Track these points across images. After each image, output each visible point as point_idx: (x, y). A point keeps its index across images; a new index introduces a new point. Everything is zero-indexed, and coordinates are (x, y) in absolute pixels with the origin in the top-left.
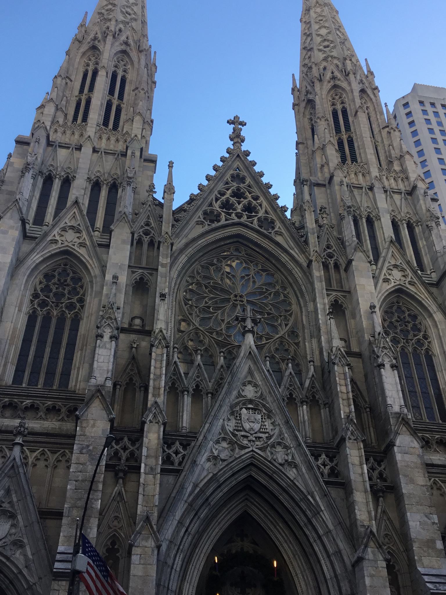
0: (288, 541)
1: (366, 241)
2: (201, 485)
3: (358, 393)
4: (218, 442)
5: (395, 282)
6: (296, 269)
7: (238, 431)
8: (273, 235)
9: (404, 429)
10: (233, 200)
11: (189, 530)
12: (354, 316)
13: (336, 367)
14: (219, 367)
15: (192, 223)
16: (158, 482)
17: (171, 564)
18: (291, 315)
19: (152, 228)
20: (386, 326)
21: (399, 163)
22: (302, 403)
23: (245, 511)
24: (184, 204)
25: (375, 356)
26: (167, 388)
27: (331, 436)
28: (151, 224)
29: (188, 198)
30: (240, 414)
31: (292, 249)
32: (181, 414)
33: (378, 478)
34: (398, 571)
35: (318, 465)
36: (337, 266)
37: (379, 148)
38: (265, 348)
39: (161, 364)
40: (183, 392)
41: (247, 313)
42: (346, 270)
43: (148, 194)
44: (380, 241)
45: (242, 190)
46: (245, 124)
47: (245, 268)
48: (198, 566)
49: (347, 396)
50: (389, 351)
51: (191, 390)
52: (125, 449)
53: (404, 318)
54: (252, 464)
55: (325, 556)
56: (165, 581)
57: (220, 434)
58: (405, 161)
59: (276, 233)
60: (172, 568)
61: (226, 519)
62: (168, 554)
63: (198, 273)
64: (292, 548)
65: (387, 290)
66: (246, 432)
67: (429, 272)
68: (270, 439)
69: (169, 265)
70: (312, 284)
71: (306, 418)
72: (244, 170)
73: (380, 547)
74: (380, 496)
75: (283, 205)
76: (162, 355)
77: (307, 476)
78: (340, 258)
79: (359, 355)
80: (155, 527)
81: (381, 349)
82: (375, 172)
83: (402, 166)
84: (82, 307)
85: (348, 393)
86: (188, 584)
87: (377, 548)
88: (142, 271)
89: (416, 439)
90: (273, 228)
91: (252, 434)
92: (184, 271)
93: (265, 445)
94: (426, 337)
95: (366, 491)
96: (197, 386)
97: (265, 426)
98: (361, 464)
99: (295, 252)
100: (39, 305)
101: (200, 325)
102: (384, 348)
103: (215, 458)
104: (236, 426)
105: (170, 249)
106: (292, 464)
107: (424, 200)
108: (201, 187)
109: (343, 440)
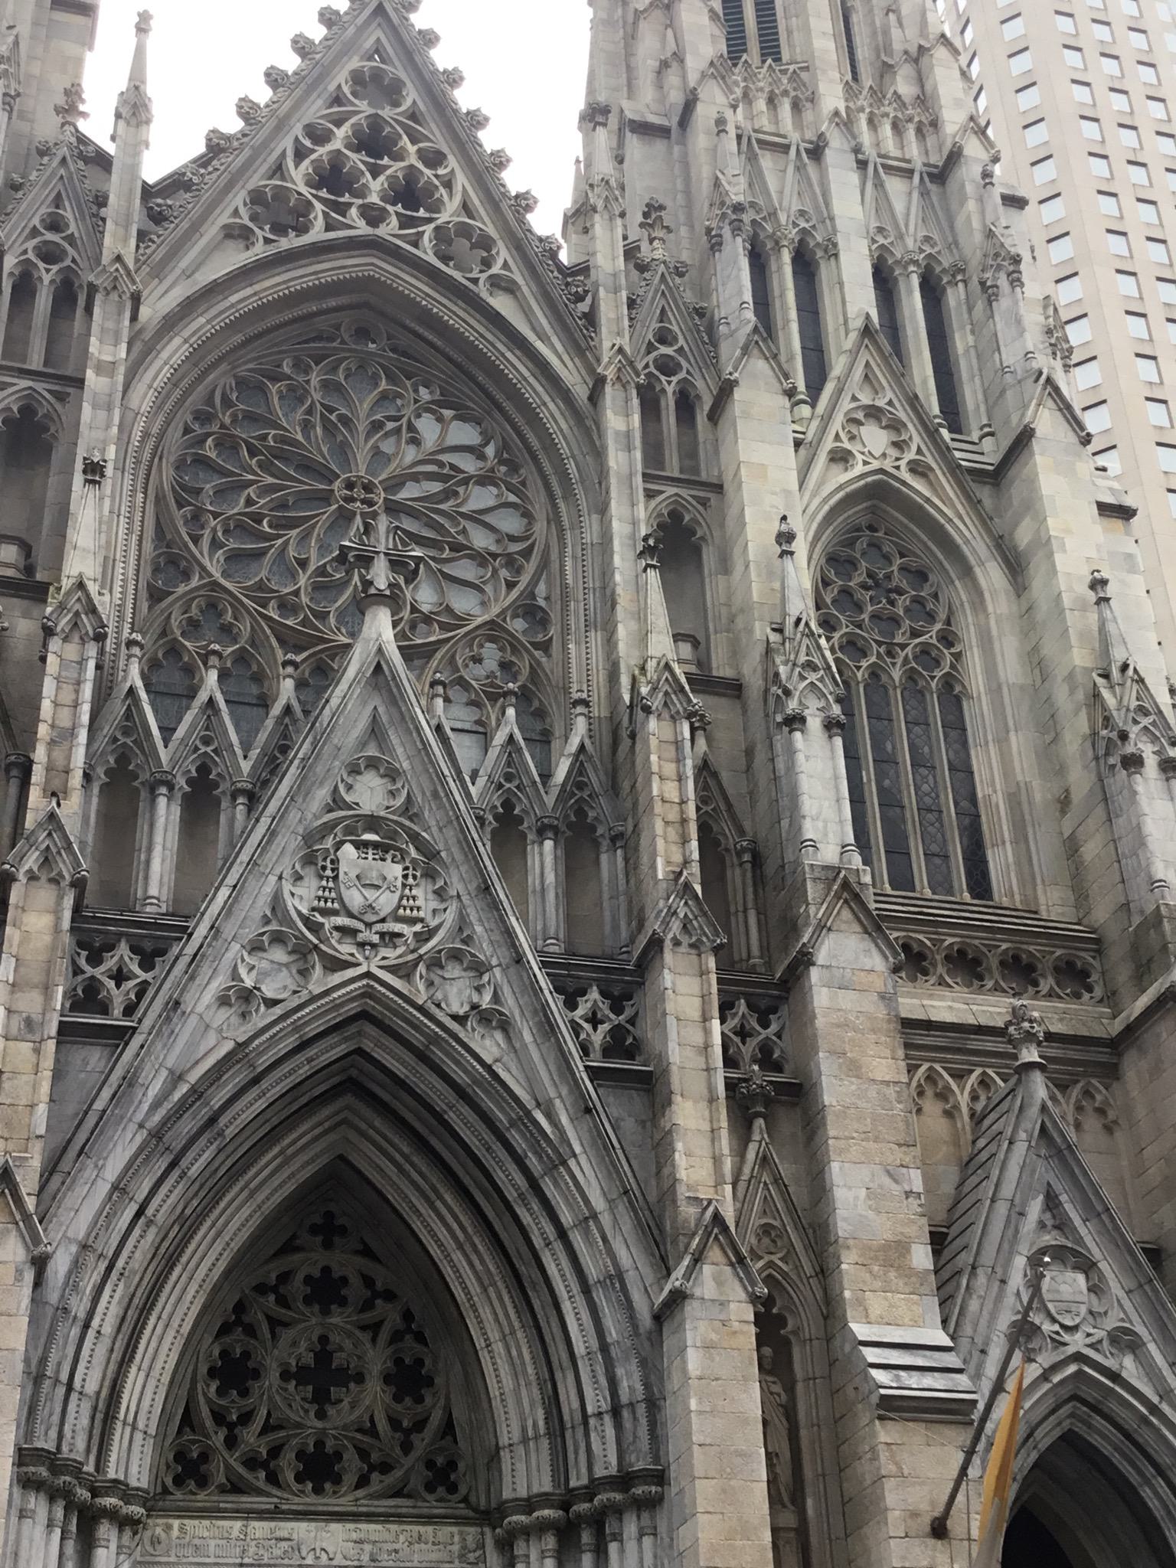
0: (468, 1248)
1: (787, 321)
2: (194, 1077)
3: (723, 807)
4: (256, 947)
5: (865, 463)
6: (551, 406)
7: (325, 912)
8: (483, 290)
9: (846, 914)
10: (357, 160)
11: (150, 1211)
12: (725, 566)
13: (653, 724)
14: (276, 710)
15: (212, 231)
16: (48, 1062)
17: (82, 1315)
18: (527, 553)
19: (71, 239)
20: (829, 601)
21: (913, 74)
22: (542, 832)
23: (342, 1158)
24: (186, 166)
25: (780, 692)
26: (100, 771)
27: (624, 934)
28: (67, 226)
29: (200, 148)
30: (335, 862)
31: (542, 337)
32: (143, 857)
33: (755, 1061)
34: (795, 1333)
35: (572, 1022)
36: (686, 403)
37: (855, 19)
38: (439, 655)
39: (77, 692)
40: (153, 790)
41: (378, 541)
42: (714, 416)
43: (60, 120)
44: (831, 328)
45: (388, 129)
47: (384, 397)
48: (175, 1323)
49: (682, 812)
50: (821, 680)
51: (181, 782)
53: (888, 577)
54: (363, 1015)
55: (576, 1288)
56: (59, 1364)
57: (267, 921)
58: (932, 68)
59: (496, 283)
60: (86, 1326)
61: (276, 1181)
62: (72, 1282)
63: (227, 403)
64: (479, 1267)
65: (840, 488)
66: (351, 915)
67: (975, 436)
68: (427, 940)
69: (121, 370)
70: (599, 454)
71: (550, 878)
72: (397, 63)
73: (739, 1261)
74: (758, 1115)
75: (523, 190)
76: (82, 663)
77: (536, 1056)
78: (697, 375)
79: (734, 689)
80: (30, 1203)
81: (798, 669)
82: (832, 97)
83: (920, 81)
85: (683, 802)
86: (142, 1374)
87: (732, 1264)
88: (30, 383)
89: (877, 945)
90: (487, 263)
91: (369, 925)
92: (178, 393)
93: (411, 957)
94: (948, 639)
95: (712, 1100)
96: (204, 769)
97: (414, 898)
98: (705, 1019)
99: (553, 352)
101: (225, 574)
102: (810, 666)
103: (247, 996)
104: (319, 899)
105: (127, 315)
106: (492, 1019)
107: (980, 200)
108: (246, 110)
109: (656, 944)
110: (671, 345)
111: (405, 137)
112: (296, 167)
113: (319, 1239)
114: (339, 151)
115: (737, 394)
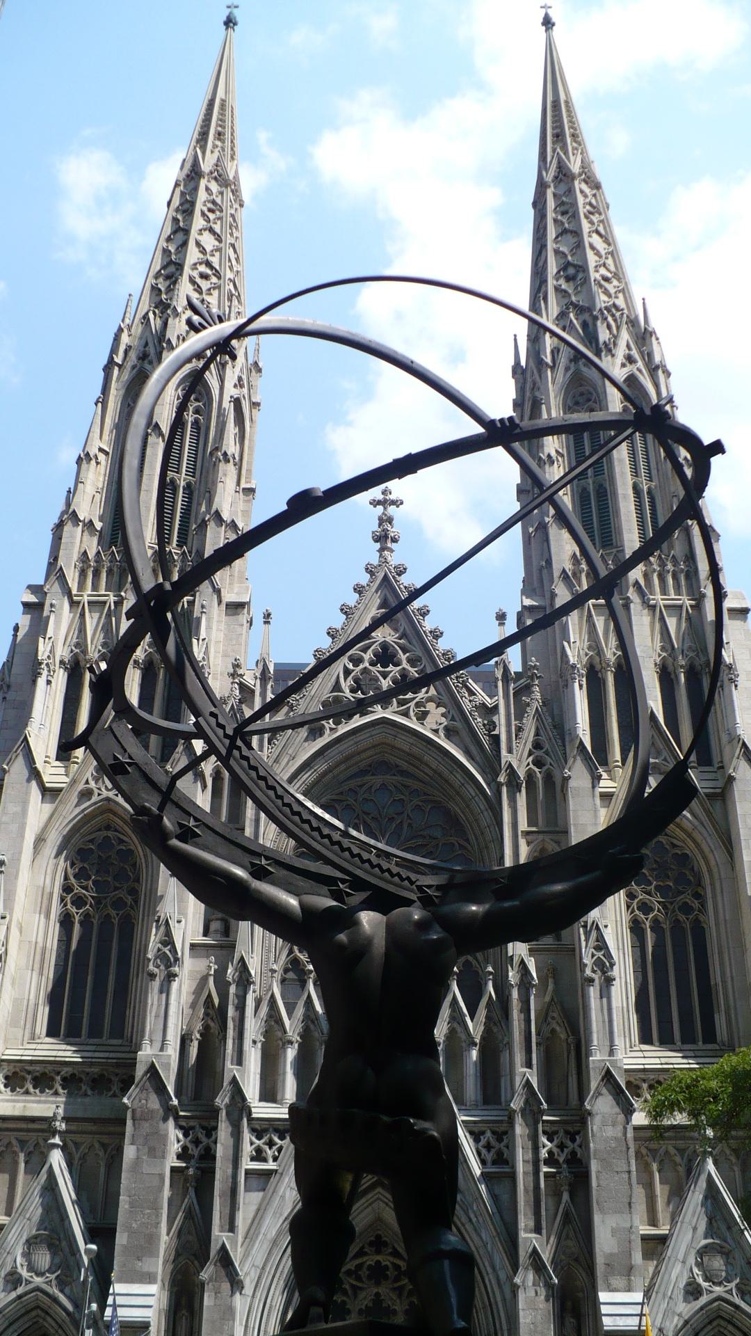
46: (402, 503)
52: (196, 1142)
84: (136, 901)
94: (697, 896)
100: (73, 903)
110: (542, 748)
111: (400, 651)
112: (345, 679)
113: (374, 1249)
114: (365, 668)
115: (572, 783)
